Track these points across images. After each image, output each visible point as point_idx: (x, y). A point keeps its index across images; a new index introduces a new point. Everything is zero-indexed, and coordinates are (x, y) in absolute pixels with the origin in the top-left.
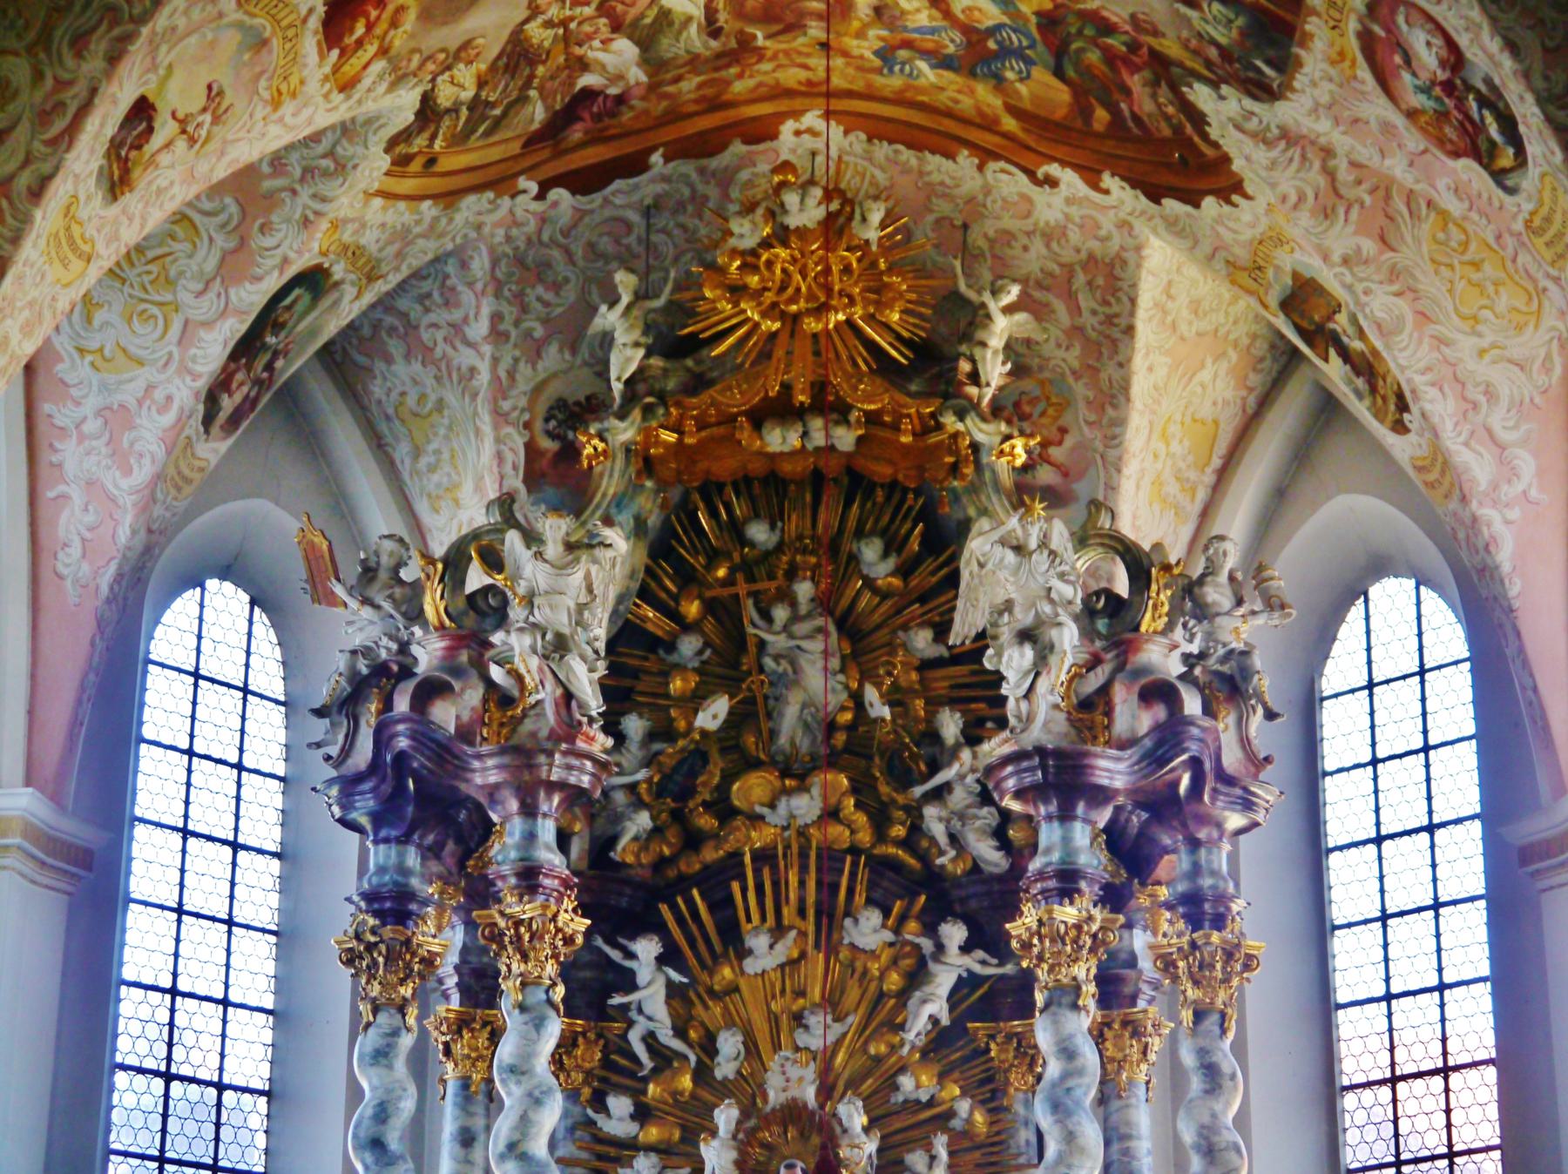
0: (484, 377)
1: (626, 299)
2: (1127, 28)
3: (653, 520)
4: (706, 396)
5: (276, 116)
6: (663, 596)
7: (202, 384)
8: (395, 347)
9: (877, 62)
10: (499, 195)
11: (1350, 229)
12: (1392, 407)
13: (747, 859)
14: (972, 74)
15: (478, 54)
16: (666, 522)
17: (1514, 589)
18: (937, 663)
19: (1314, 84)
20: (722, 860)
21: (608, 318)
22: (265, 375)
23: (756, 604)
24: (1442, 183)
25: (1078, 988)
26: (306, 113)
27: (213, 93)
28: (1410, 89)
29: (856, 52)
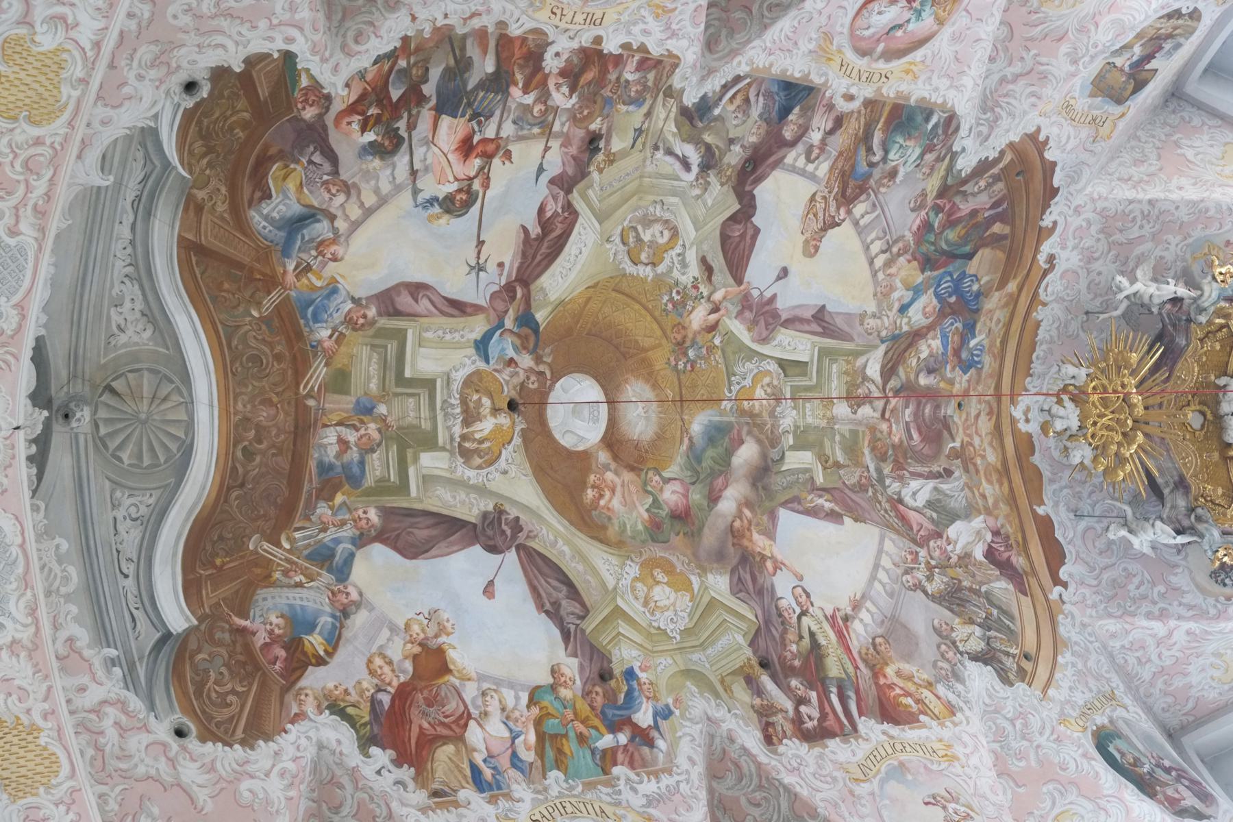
0: (1192, 625)
1: (1123, 533)
2: (923, 213)
5: (963, 759)
8: (1178, 682)
9: (973, 371)
12: (1180, 22)
14: (977, 311)
15: (947, 624)
19: (936, 89)
22: (1174, 773)
26: (966, 738)
28: (920, 24)
29: (964, 385)
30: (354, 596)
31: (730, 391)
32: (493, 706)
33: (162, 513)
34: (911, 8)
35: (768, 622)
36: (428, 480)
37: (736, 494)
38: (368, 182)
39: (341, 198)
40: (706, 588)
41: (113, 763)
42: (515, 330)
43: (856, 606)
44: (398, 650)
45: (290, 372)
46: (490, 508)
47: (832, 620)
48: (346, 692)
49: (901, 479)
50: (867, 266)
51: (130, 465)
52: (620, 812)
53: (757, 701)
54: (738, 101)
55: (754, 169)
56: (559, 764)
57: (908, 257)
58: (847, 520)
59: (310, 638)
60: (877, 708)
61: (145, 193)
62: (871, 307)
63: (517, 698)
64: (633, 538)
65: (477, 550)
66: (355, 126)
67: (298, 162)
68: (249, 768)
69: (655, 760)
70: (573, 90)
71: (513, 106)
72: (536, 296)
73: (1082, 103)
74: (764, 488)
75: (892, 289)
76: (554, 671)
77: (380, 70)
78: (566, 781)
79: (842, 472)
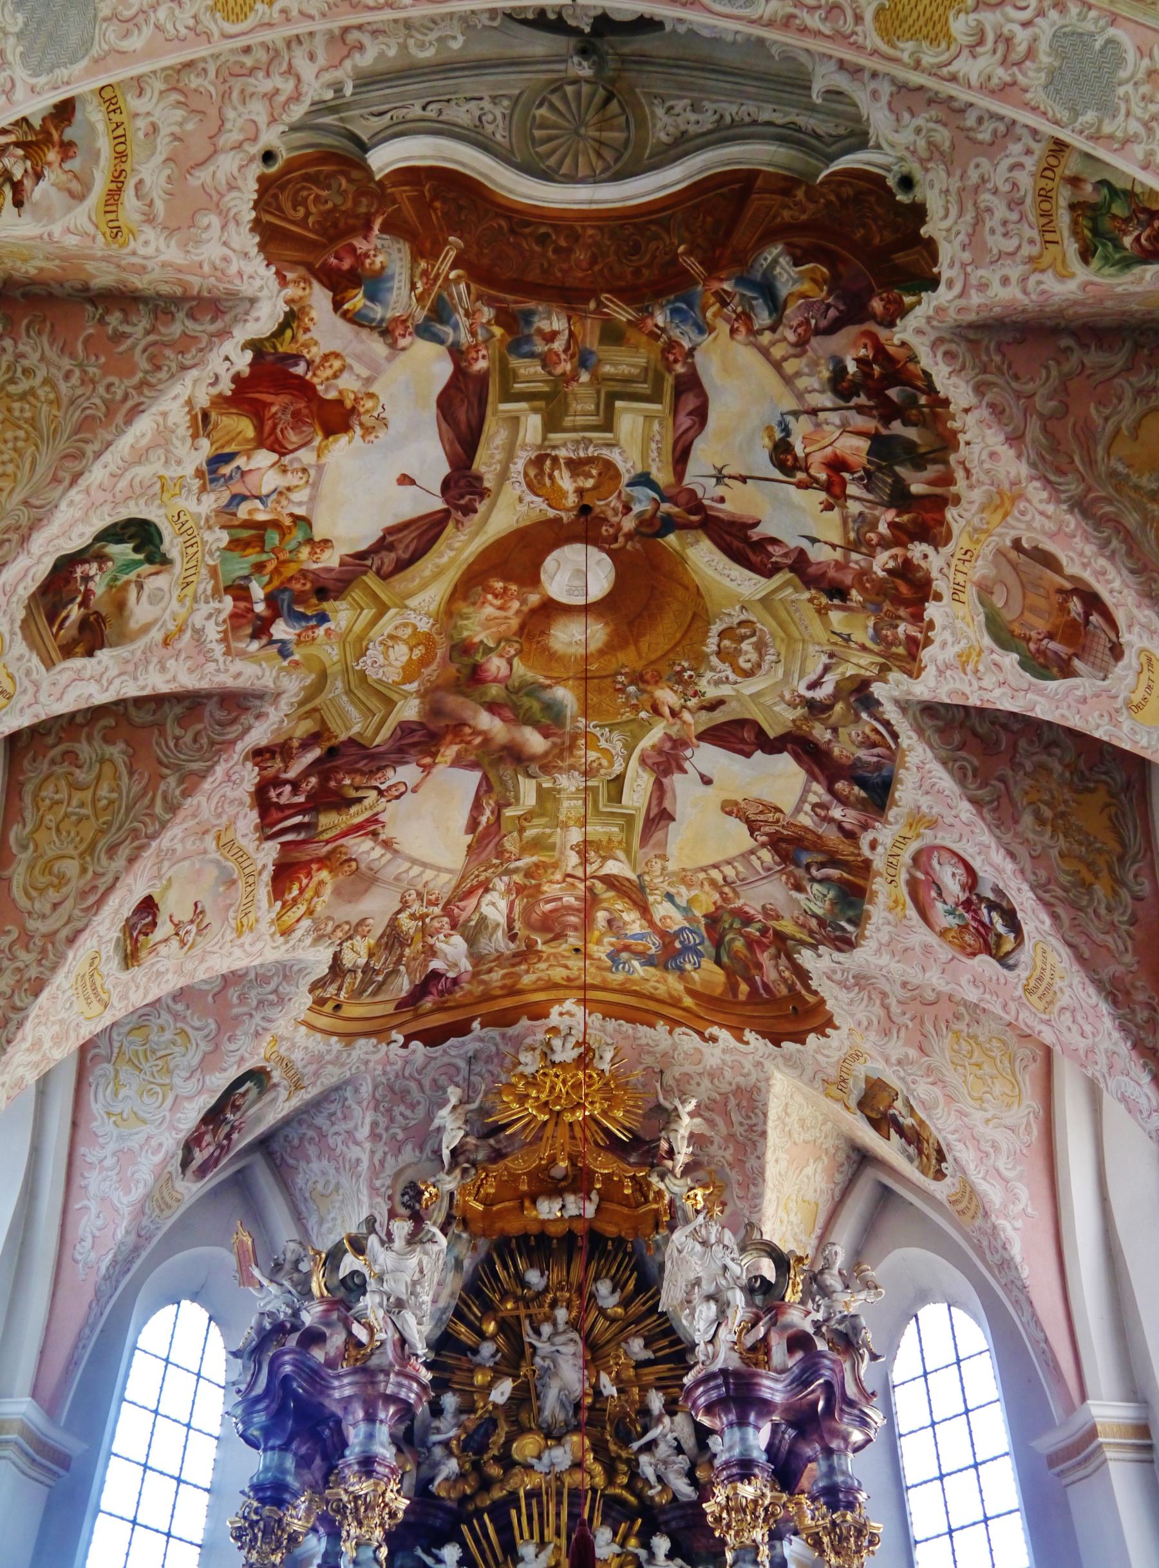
0: (365, 1164)
1: (454, 1101)
2: (760, 917)
3: (467, 1263)
4: (501, 1164)
5: (238, 942)
6: (472, 1317)
7: (182, 1136)
8: (312, 1151)
9: (609, 963)
10: (379, 1042)
11: (901, 1043)
12: (934, 1162)
13: (522, 1493)
14: (666, 968)
16: (475, 1269)
17: (1025, 1273)
18: (648, 1363)
20: (504, 1497)
21: (444, 1116)
23: (531, 1323)
24: (964, 981)
25: (757, 1548)
26: (259, 945)
27: (198, 911)
28: (941, 913)
29: (596, 955)
30: (402, 342)
31: (595, 727)
32: (291, 479)
33: (485, 145)
34: (957, 905)
35: (373, 757)
36: (514, 421)
37: (495, 730)
38: (807, 365)
39: (792, 337)
40: (406, 698)
41: (237, 84)
42: (659, 514)
43: (387, 844)
44: (348, 384)
45: (622, 283)
46: (487, 484)
47: (374, 820)
48: (307, 330)
49: (508, 891)
50: (711, 862)
51: (534, 117)
52: (188, 601)
53: (295, 743)
54: (874, 737)
55: (806, 752)
56: (236, 544)
57: (720, 902)
58: (469, 838)
59: (360, 295)
60: (287, 860)
61: (802, 136)
62: (672, 866)
63: (300, 504)
64: (455, 627)
65: (445, 469)
66: (862, 352)
67: (829, 293)
68: (232, 225)
69: (238, 639)
70: (890, 572)
71: (877, 513)
72: (690, 536)
73: (861, 1070)
74: (501, 758)
75: (689, 886)
76: (326, 543)
77: (917, 377)
78: (218, 549)
79: (515, 834)
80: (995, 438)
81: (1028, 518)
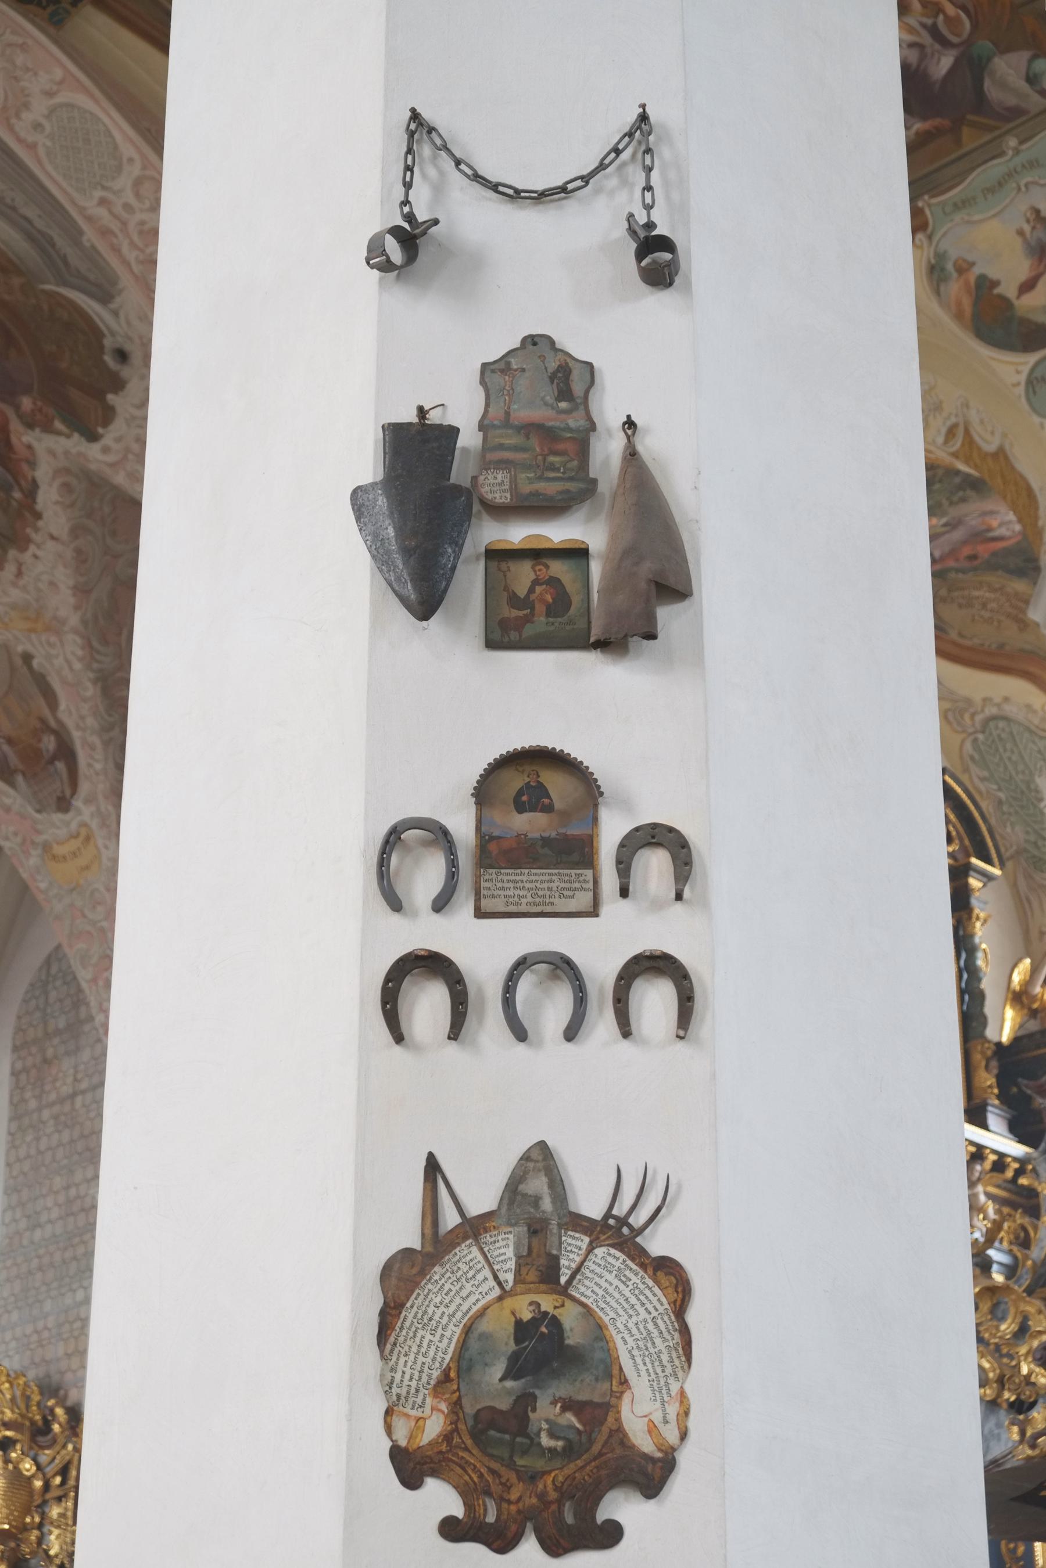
80: (64, 577)
81: (53, 652)
